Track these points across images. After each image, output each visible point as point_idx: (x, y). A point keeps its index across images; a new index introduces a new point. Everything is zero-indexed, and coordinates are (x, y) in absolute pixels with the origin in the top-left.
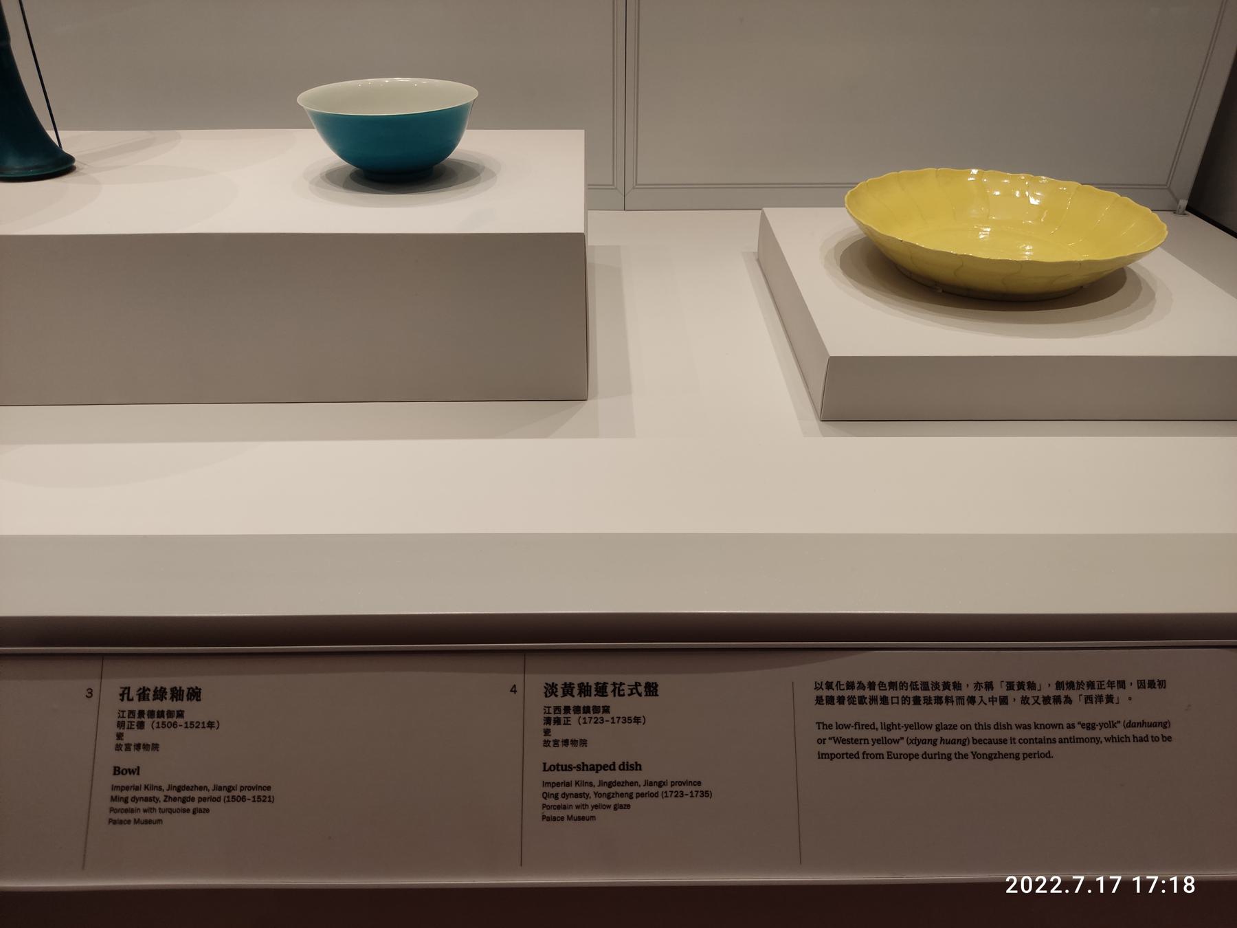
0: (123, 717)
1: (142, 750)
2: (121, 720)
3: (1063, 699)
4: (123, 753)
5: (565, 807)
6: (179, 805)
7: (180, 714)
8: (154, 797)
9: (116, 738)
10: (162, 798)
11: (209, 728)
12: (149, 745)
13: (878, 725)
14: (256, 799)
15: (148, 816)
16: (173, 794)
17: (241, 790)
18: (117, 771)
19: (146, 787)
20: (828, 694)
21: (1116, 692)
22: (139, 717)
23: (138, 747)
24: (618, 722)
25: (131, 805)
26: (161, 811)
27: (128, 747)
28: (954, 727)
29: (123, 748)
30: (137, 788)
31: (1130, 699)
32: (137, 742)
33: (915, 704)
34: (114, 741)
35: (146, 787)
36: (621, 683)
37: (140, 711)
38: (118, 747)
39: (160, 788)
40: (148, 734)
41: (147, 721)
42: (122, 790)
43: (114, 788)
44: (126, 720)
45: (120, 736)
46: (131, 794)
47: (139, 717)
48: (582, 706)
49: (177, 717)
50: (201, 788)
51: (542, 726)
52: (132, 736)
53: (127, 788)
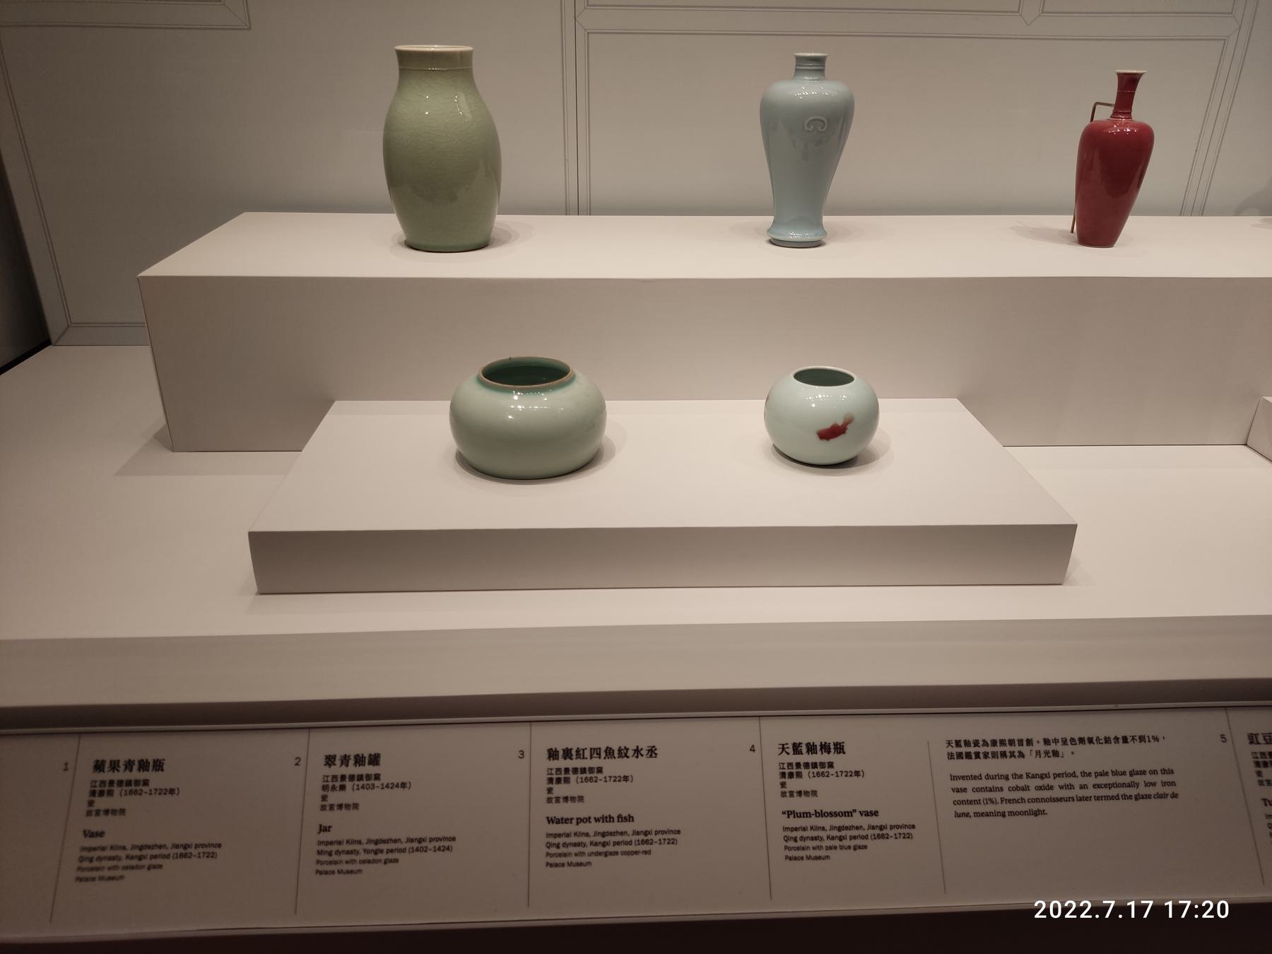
0: (552, 774)
2: (550, 776)
3: (1008, 754)
4: (554, 805)
5: (803, 849)
7: (600, 770)
9: (547, 792)
10: (588, 844)
13: (1078, 774)
15: (579, 859)
16: (599, 839)
19: (575, 834)
20: (963, 750)
21: (1025, 749)
24: (155, 793)
25: (562, 850)
26: (591, 854)
28: (1124, 773)
30: (568, 835)
31: (1073, 753)
32: (565, 796)
33: (976, 758)
34: (546, 795)
35: (575, 834)
37: (565, 769)
38: (549, 800)
39: (587, 835)
41: (573, 777)
44: (555, 777)
45: (550, 790)
46: (561, 840)
49: (597, 772)
50: (622, 834)
52: (560, 790)
53: (559, 835)
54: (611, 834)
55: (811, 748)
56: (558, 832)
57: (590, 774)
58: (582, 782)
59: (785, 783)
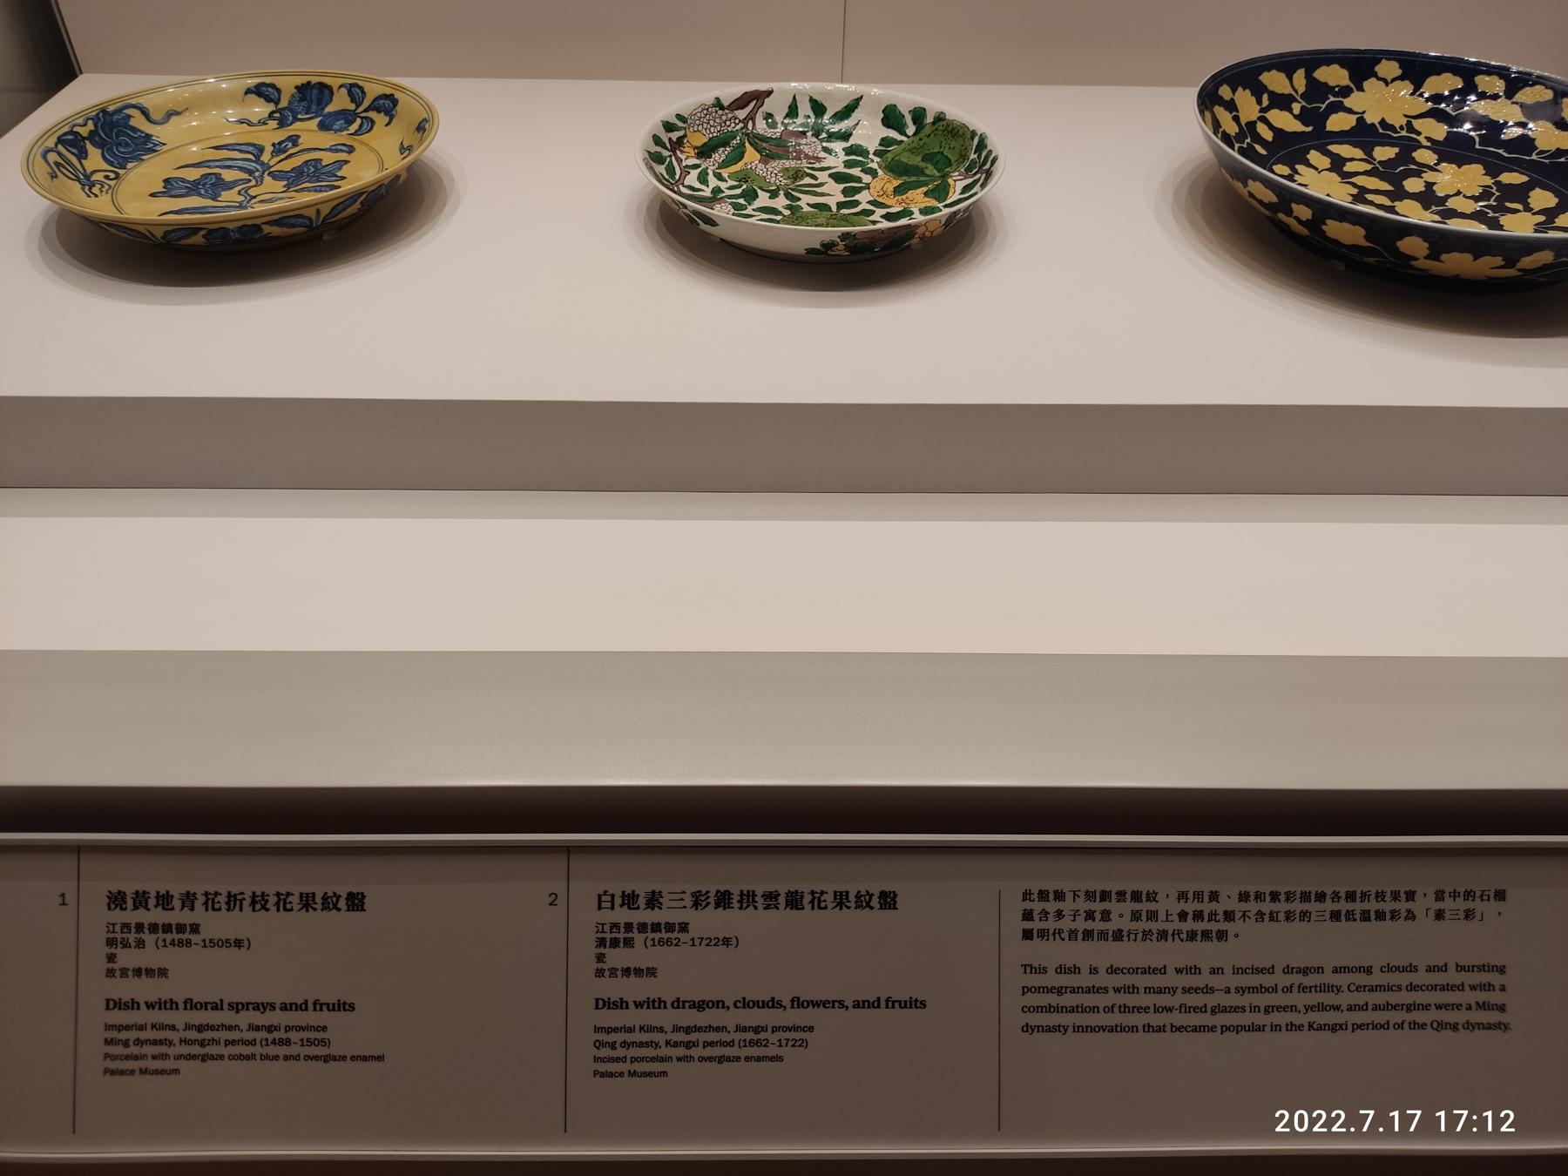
1: (144, 976)
6: (196, 1050)
8: (652, 1042)
11: (237, 948)
12: (154, 970)
14: (305, 1043)
17: (286, 1031)
18: (114, 1004)
22: (137, 932)
23: (138, 972)
27: (124, 972)
29: (118, 974)
32: (137, 967)
36: (822, 891)
38: (110, 973)
40: (150, 956)
42: (119, 1031)
43: (108, 1027)
45: (111, 958)
47: (137, 932)
48: (650, 923)
51: (594, 951)
54: (211, 1028)
55: (164, 900)
56: (125, 1023)
57: (182, 935)
58: (654, 945)
59: (603, 955)
